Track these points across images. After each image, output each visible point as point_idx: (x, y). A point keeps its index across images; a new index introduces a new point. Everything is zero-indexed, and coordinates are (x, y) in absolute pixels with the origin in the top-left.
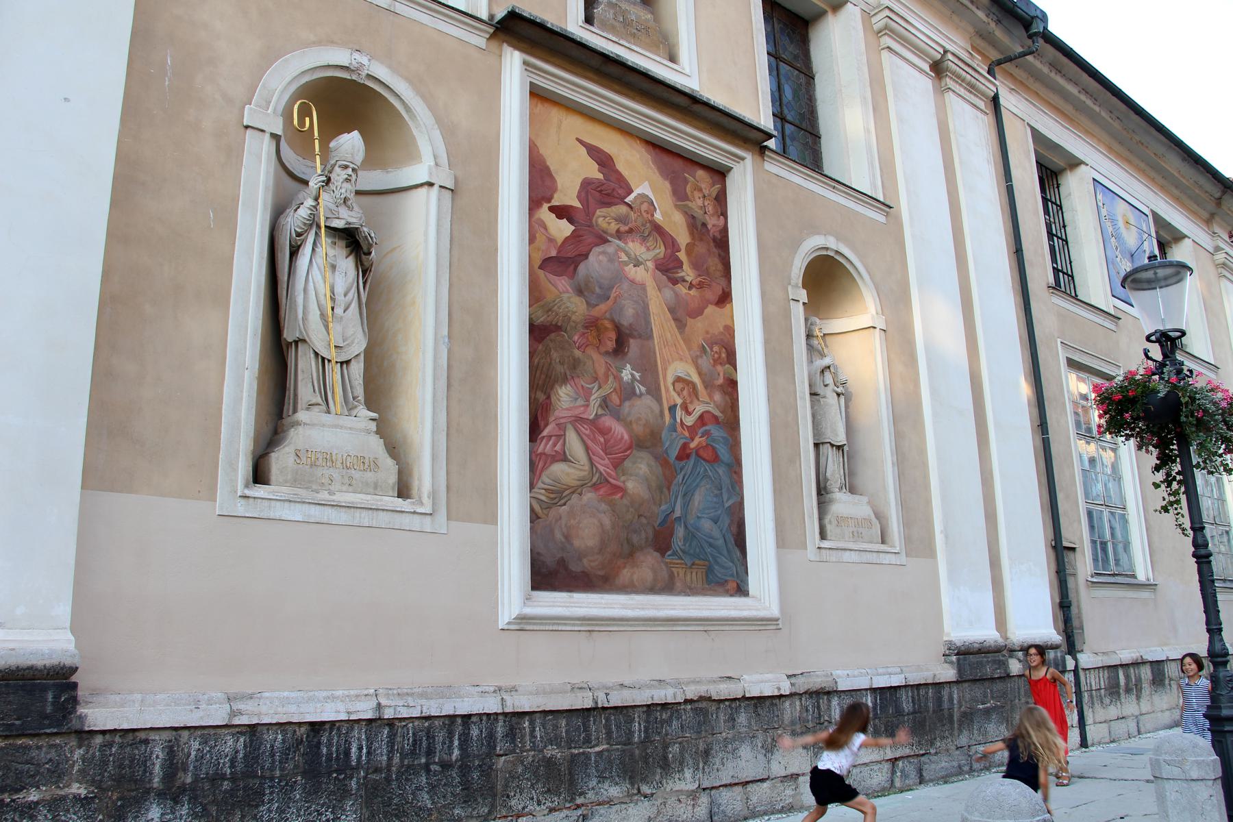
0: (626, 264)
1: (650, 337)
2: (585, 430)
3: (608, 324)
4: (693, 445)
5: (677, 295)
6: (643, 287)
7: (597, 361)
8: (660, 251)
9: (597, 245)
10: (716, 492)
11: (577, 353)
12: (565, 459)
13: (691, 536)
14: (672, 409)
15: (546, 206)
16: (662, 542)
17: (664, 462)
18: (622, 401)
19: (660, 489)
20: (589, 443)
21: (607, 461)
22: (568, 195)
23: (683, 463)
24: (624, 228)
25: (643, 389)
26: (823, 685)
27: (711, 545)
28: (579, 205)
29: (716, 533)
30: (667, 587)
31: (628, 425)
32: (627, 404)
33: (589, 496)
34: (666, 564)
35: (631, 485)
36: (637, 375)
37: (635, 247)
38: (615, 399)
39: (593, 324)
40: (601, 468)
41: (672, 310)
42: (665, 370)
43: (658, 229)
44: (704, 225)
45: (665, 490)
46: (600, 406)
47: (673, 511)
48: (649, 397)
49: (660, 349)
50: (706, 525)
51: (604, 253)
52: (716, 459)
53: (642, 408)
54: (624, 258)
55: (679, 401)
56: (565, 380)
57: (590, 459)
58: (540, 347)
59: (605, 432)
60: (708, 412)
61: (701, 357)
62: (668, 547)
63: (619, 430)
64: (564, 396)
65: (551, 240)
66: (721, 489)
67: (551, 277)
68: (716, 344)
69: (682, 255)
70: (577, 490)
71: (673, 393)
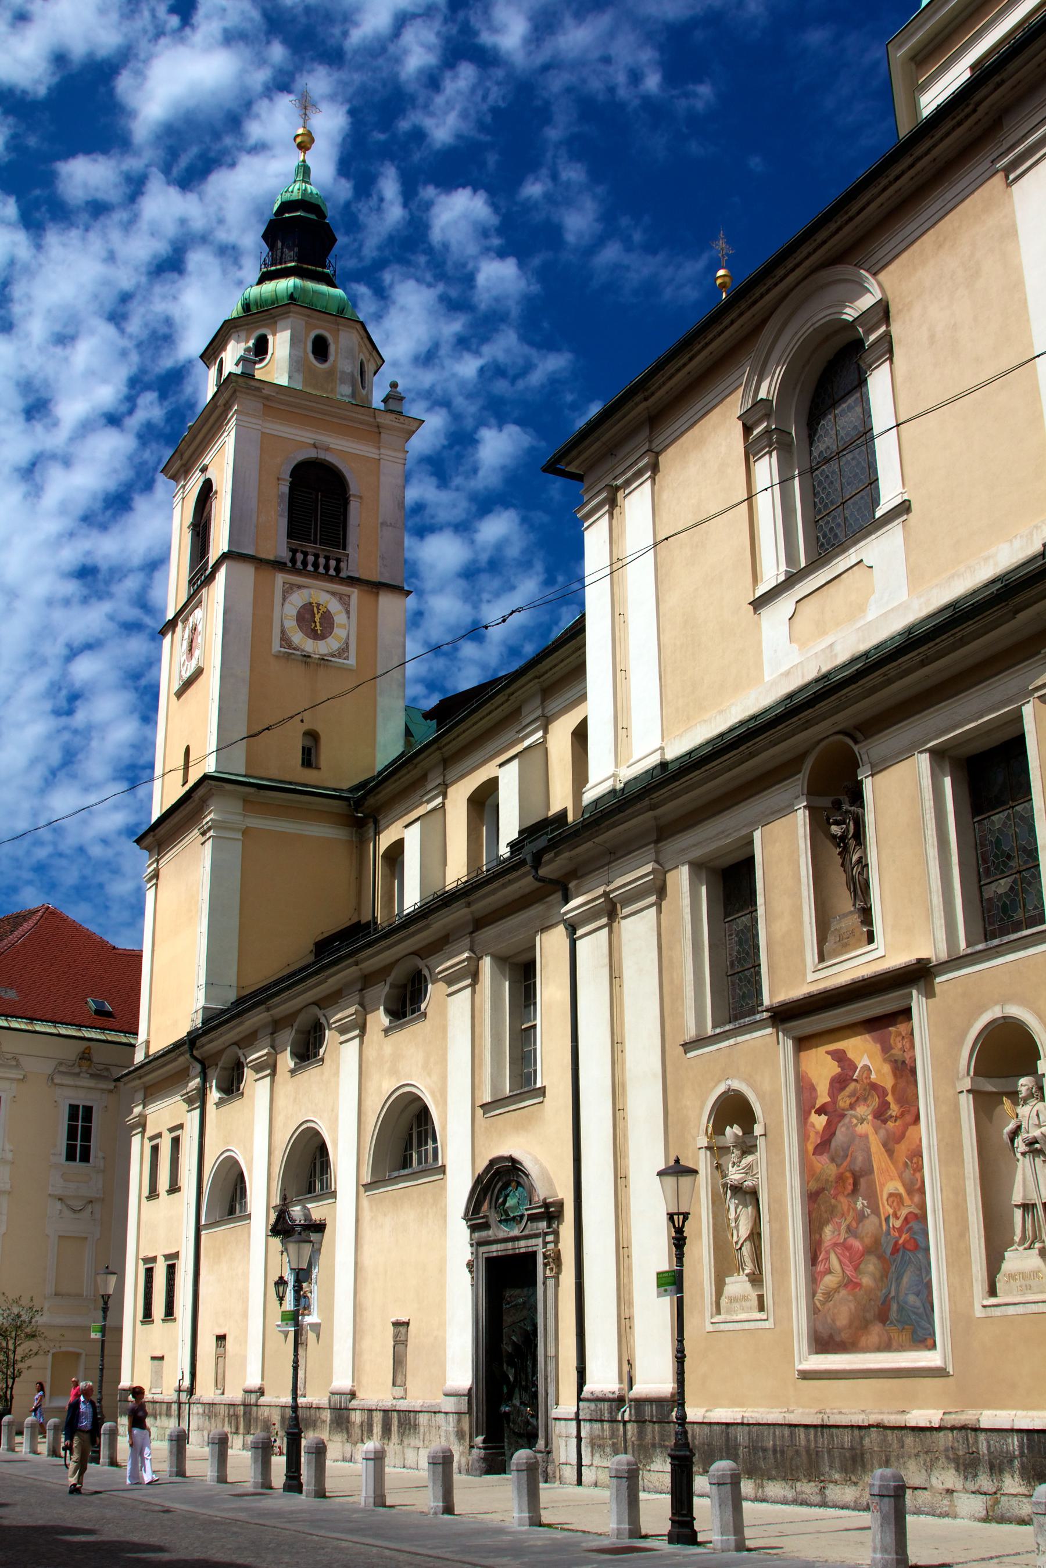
0: (856, 1125)
1: (871, 1171)
2: (839, 1251)
3: (848, 1174)
4: (901, 1242)
5: (887, 1131)
6: (866, 1136)
7: (844, 1201)
8: (875, 1102)
9: (839, 1122)
10: (918, 1273)
11: (833, 1201)
12: (829, 1271)
13: (901, 1309)
14: (887, 1219)
15: (813, 1111)
16: (883, 1317)
17: (881, 1257)
18: (858, 1224)
19: (882, 1277)
20: (842, 1258)
21: (851, 1268)
22: (823, 1097)
23: (895, 1257)
24: (854, 1099)
25: (869, 1211)
26: (967, 1422)
27: (915, 1313)
28: (828, 1099)
29: (918, 1304)
30: (886, 1347)
31: (861, 1240)
32: (861, 1225)
33: (843, 1292)
34: (886, 1330)
35: (866, 1281)
36: (865, 1202)
37: (862, 1110)
38: (854, 1224)
39: (840, 1178)
40: (848, 1273)
41: (885, 1145)
42: (882, 1191)
43: (874, 1086)
44: (904, 1062)
45: (885, 1279)
46: (846, 1232)
47: (889, 1293)
48: (873, 1216)
49: (879, 1178)
50: (912, 1299)
51: (843, 1125)
52: (917, 1247)
53: (870, 1225)
54: (855, 1121)
55: (891, 1211)
56: (827, 1222)
57: (842, 1269)
58: (816, 1206)
59: (848, 1248)
60: (911, 1213)
61: (905, 1171)
62: (887, 1319)
63: (857, 1244)
64: (828, 1232)
65: (817, 1133)
66: (920, 1270)
67: (818, 1157)
68: (915, 1156)
69: (890, 1098)
70: (837, 1290)
71: (888, 1207)
